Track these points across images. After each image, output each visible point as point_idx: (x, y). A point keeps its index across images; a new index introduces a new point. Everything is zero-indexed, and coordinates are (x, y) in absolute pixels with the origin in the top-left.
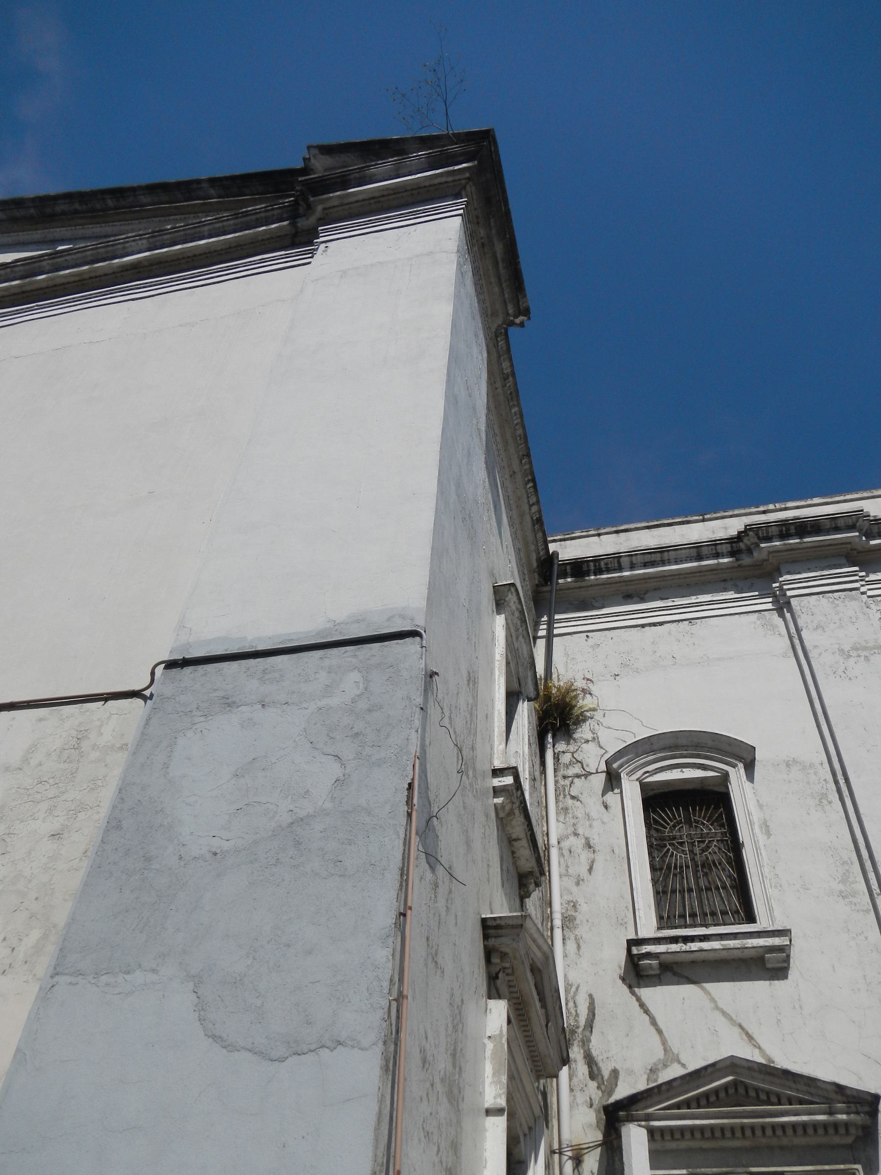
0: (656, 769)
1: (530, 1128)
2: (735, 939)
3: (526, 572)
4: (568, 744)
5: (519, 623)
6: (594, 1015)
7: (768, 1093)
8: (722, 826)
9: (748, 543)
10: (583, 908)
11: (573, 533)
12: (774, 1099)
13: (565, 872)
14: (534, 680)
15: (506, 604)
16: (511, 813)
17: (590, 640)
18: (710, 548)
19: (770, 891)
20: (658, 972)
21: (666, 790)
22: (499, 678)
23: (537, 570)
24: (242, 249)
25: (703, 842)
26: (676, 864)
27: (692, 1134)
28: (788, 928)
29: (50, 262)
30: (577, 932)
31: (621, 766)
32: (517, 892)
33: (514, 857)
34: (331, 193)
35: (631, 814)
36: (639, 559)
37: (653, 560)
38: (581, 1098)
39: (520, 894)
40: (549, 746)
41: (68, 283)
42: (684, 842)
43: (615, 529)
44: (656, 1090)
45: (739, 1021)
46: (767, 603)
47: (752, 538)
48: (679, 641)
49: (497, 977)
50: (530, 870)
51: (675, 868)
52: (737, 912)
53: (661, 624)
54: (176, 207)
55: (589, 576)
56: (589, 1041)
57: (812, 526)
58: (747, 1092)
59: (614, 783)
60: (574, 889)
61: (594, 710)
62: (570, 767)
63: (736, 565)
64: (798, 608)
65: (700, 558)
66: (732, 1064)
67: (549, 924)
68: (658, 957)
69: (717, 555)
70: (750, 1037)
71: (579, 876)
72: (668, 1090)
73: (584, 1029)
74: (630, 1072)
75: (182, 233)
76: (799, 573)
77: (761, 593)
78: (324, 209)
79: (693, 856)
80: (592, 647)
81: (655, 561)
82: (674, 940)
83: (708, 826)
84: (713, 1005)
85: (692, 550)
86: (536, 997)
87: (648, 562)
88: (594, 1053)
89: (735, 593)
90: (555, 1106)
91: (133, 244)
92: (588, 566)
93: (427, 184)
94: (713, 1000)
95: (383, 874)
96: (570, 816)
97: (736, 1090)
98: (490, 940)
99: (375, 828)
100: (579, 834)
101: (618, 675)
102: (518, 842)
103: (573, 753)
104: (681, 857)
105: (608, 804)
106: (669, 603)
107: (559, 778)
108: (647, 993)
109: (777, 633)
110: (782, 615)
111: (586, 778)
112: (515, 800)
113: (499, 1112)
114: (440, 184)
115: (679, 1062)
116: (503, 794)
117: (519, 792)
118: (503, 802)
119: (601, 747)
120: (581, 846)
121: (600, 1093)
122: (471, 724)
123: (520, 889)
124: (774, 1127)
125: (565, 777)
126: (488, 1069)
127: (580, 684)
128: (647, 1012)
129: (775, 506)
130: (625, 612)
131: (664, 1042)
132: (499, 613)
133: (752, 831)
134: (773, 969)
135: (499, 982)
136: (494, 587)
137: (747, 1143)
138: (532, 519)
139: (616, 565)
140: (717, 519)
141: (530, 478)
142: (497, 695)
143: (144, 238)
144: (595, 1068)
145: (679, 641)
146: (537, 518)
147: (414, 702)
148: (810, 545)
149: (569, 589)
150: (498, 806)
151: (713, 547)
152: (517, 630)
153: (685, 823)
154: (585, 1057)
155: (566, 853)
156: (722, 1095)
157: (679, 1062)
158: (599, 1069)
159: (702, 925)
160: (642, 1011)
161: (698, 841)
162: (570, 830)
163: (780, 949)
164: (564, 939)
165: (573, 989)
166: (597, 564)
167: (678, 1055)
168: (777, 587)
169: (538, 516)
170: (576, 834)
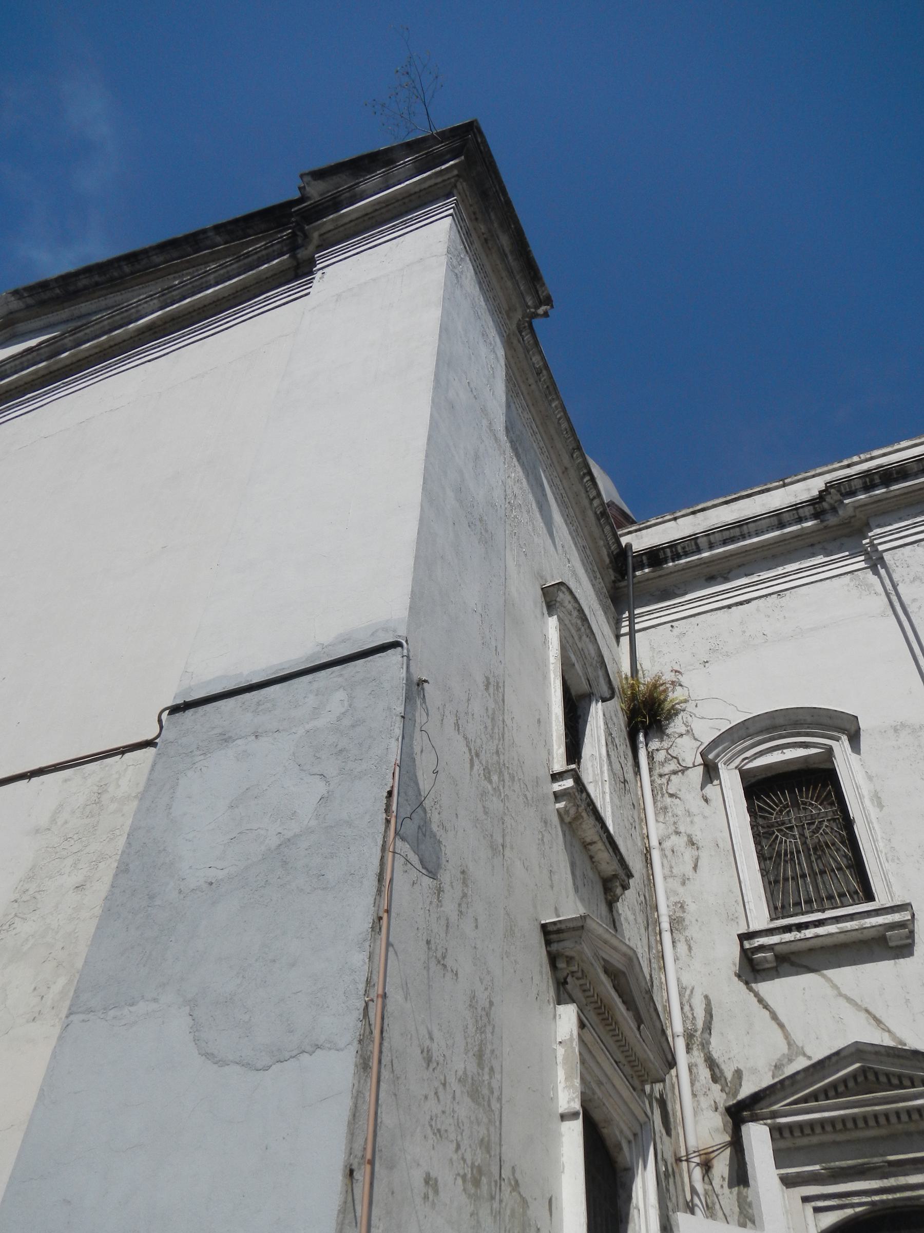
0: (755, 754)
1: (635, 1135)
2: (852, 920)
3: (596, 569)
4: (662, 740)
5: (579, 622)
6: (711, 1016)
7: (900, 1077)
8: (832, 804)
9: (832, 502)
10: (691, 907)
11: (649, 521)
12: (907, 1082)
13: (670, 873)
14: (607, 679)
15: (558, 604)
16: (578, 817)
17: (675, 630)
18: (791, 513)
19: (886, 866)
20: (774, 964)
21: (769, 775)
22: (554, 681)
23: (610, 565)
24: (248, 291)
25: (813, 823)
26: (786, 851)
27: (823, 1128)
28: (908, 901)
29: (71, 338)
30: (687, 933)
31: (718, 756)
32: (602, 897)
33: (593, 862)
34: (325, 217)
35: (732, 803)
36: (718, 537)
37: (732, 535)
38: (705, 1103)
39: (606, 899)
40: (641, 745)
41: (91, 356)
42: (793, 827)
43: (691, 510)
44: (779, 1086)
45: (865, 1005)
46: (859, 562)
47: (834, 496)
48: (769, 617)
49: (565, 982)
50: (614, 873)
51: (786, 854)
52: (856, 892)
53: (748, 601)
54: (188, 261)
55: (667, 563)
56: (709, 1043)
57: (898, 473)
58: (877, 1079)
59: (712, 775)
60: (681, 890)
61: (686, 701)
62: (666, 765)
63: (821, 526)
64: (892, 562)
65: (782, 526)
66: (858, 1051)
67: (658, 928)
68: (773, 949)
69: (800, 520)
70: (878, 1021)
71: (684, 875)
72: (792, 1084)
73: (702, 1032)
74: (754, 1071)
75: (190, 286)
76: (890, 524)
77: (851, 552)
78: (321, 235)
79: (803, 839)
80: (678, 637)
81: (734, 537)
82: (788, 929)
83: (816, 807)
84: (836, 992)
85: (772, 519)
86: (618, 1001)
87: (727, 539)
88: (715, 1055)
89: (824, 557)
90: (679, 1114)
91: (145, 305)
92: (665, 553)
93: (417, 189)
94: (835, 987)
95: (361, 882)
96: (670, 814)
97: (866, 1077)
98: (552, 945)
99: (355, 839)
100: (680, 833)
101: (707, 662)
102: (594, 845)
103: (667, 750)
104: (791, 843)
105: (708, 797)
106: (755, 578)
107: (656, 777)
108: (765, 988)
109: (873, 592)
110: (876, 573)
111: (683, 773)
112: (579, 803)
113: (574, 1115)
114: (430, 187)
115: (804, 1055)
116: (565, 798)
117: (584, 795)
118: (566, 806)
119: (696, 739)
120: (683, 844)
121: (724, 1095)
122: (493, 729)
123: (605, 893)
124: (909, 1111)
125: (661, 776)
126: (561, 1074)
127: (668, 677)
128: (766, 1007)
129: (860, 458)
130: (709, 595)
131: (787, 1036)
132: (550, 615)
133: (863, 805)
134: (897, 947)
135: (569, 987)
136: (542, 589)
137: (883, 1132)
138: (596, 513)
139: (694, 547)
140: (798, 481)
141: (585, 471)
142: (554, 699)
143: (155, 298)
144: (717, 1071)
145: (769, 617)
146: (601, 512)
147: (394, 711)
148: (897, 493)
149: (648, 580)
150: (560, 810)
151: (795, 512)
152: (579, 630)
153: (792, 807)
154: (705, 1061)
155: (669, 853)
156: (851, 1084)
157: (804, 1055)
158: (721, 1071)
159: (818, 911)
160: (761, 1006)
161: (807, 824)
162: (672, 829)
163: (901, 925)
164: (673, 942)
165: (688, 992)
166: (674, 550)
167: (802, 1048)
168: (868, 543)
169: (601, 509)
170: (678, 833)
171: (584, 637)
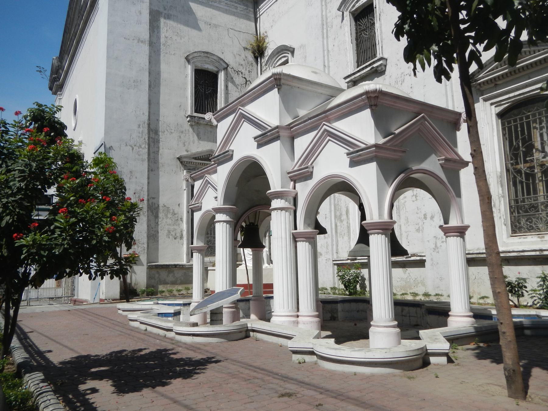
132: (189, 65)
171: (210, 57)
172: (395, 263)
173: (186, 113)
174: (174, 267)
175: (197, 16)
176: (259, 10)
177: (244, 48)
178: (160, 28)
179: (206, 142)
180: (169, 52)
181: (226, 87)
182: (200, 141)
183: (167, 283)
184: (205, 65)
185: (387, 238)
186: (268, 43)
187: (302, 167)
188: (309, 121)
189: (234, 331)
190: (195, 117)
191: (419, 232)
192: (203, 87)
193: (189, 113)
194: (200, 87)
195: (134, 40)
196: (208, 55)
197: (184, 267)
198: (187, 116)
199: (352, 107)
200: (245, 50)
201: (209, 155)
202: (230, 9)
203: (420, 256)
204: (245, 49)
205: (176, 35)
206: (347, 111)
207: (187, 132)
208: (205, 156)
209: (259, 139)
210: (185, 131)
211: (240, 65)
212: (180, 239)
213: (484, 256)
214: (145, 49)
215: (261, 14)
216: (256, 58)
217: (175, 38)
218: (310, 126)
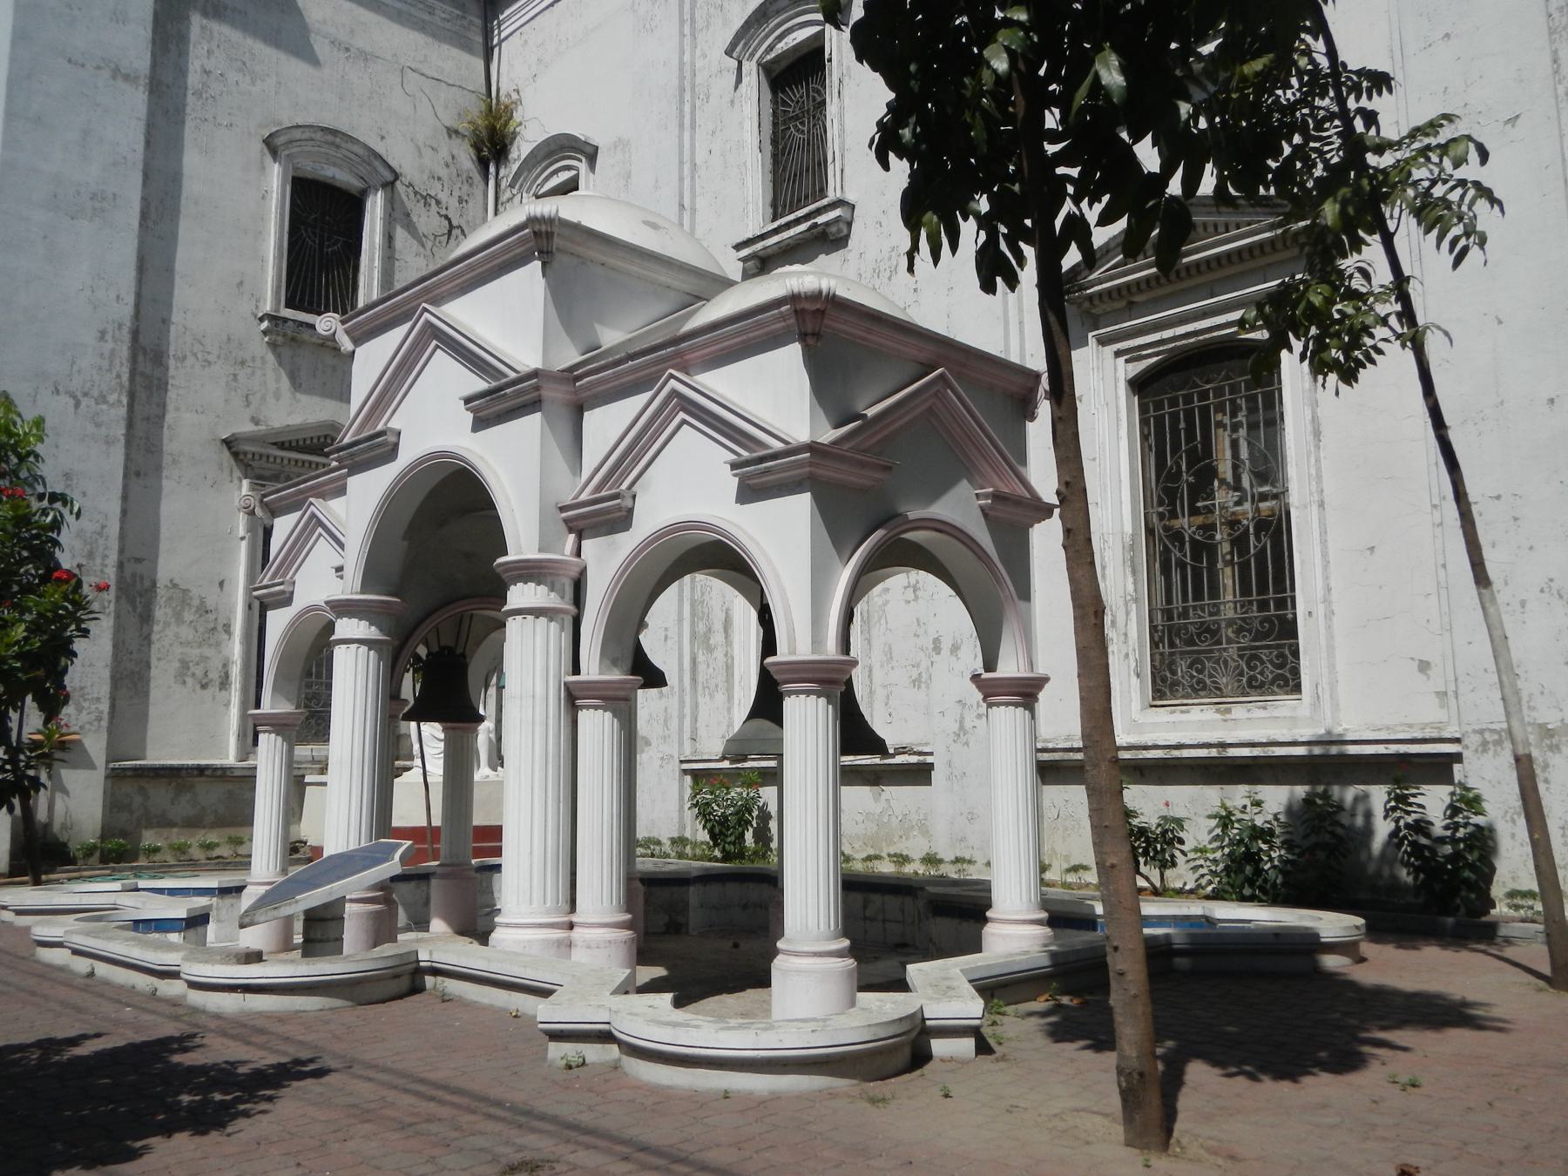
171: (343, 145)
172: (852, 771)
173: (257, 307)
174: (196, 772)
175: (307, 20)
176: (499, 26)
177: (448, 129)
178: (189, 41)
179: (316, 399)
180: (215, 118)
181: (389, 239)
182: (298, 395)
183: (171, 824)
184: (325, 166)
185: (830, 707)
186: (520, 124)
187: (603, 493)
188: (630, 363)
189: (376, 975)
190: (285, 320)
191: (919, 687)
192: (315, 234)
193: (267, 307)
194: (306, 231)
195: (98, 68)
196: (338, 140)
197: (228, 773)
198: (260, 315)
199: (751, 335)
200: (450, 137)
201: (326, 437)
202: (413, 10)
203: (920, 754)
204: (452, 132)
205: (240, 70)
206: (737, 344)
207: (258, 363)
208: (312, 439)
209: (480, 404)
210: (253, 359)
211: (433, 177)
212: (220, 690)
213: (1079, 756)
214: (137, 100)
215: (503, 35)
216: (483, 164)
217: (233, 76)
218: (632, 377)
